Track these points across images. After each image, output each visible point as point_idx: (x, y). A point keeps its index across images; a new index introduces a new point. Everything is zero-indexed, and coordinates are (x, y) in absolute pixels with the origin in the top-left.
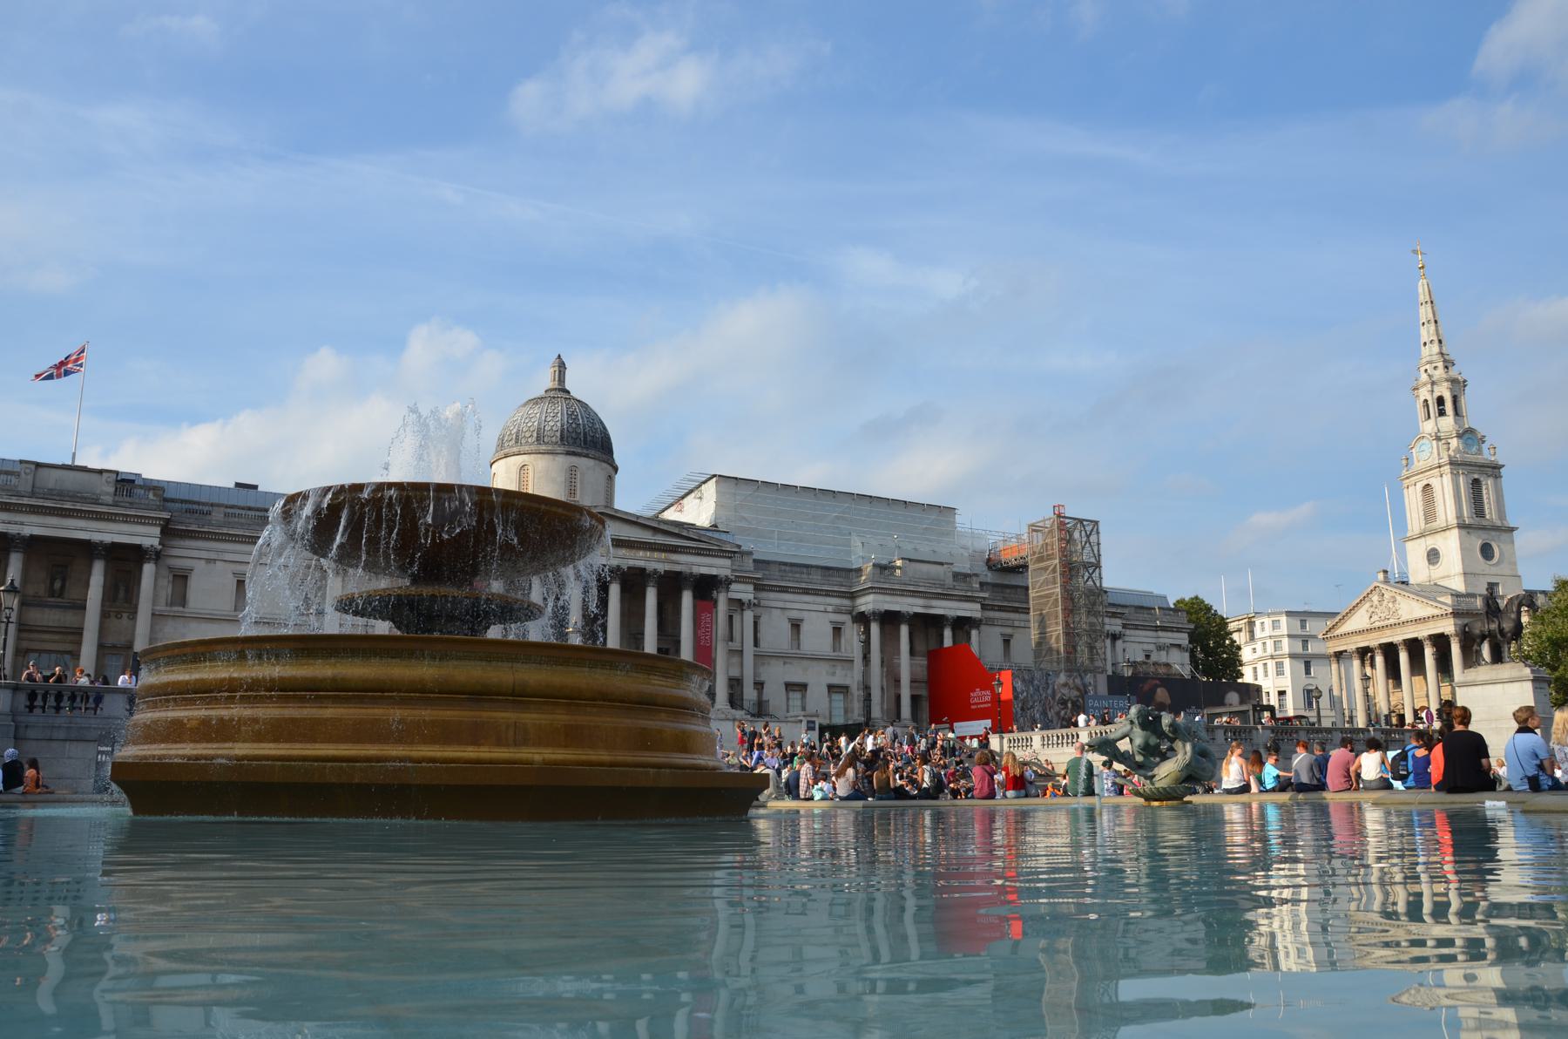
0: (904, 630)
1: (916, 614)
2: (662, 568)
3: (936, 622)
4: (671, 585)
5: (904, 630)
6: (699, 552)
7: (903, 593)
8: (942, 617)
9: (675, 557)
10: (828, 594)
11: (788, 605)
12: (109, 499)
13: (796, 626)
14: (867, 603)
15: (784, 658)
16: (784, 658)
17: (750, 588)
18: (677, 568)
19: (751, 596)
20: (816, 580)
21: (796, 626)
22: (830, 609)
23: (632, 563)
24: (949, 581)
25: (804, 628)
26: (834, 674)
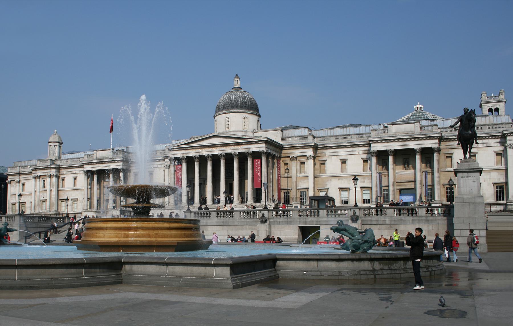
0: (391, 159)
1: (396, 151)
2: (237, 152)
3: (412, 152)
4: (243, 157)
5: (391, 159)
6: (251, 143)
7: (387, 141)
8: (413, 149)
9: (242, 147)
10: (359, 146)
11: (340, 154)
12: (111, 157)
13: (344, 162)
14: (375, 147)
15: (338, 177)
16: (338, 177)
17: (311, 150)
18: (244, 151)
19: (312, 154)
20: (354, 140)
21: (344, 162)
22: (361, 152)
23: (227, 152)
24: (418, 130)
25: (348, 162)
26: (364, 182)
